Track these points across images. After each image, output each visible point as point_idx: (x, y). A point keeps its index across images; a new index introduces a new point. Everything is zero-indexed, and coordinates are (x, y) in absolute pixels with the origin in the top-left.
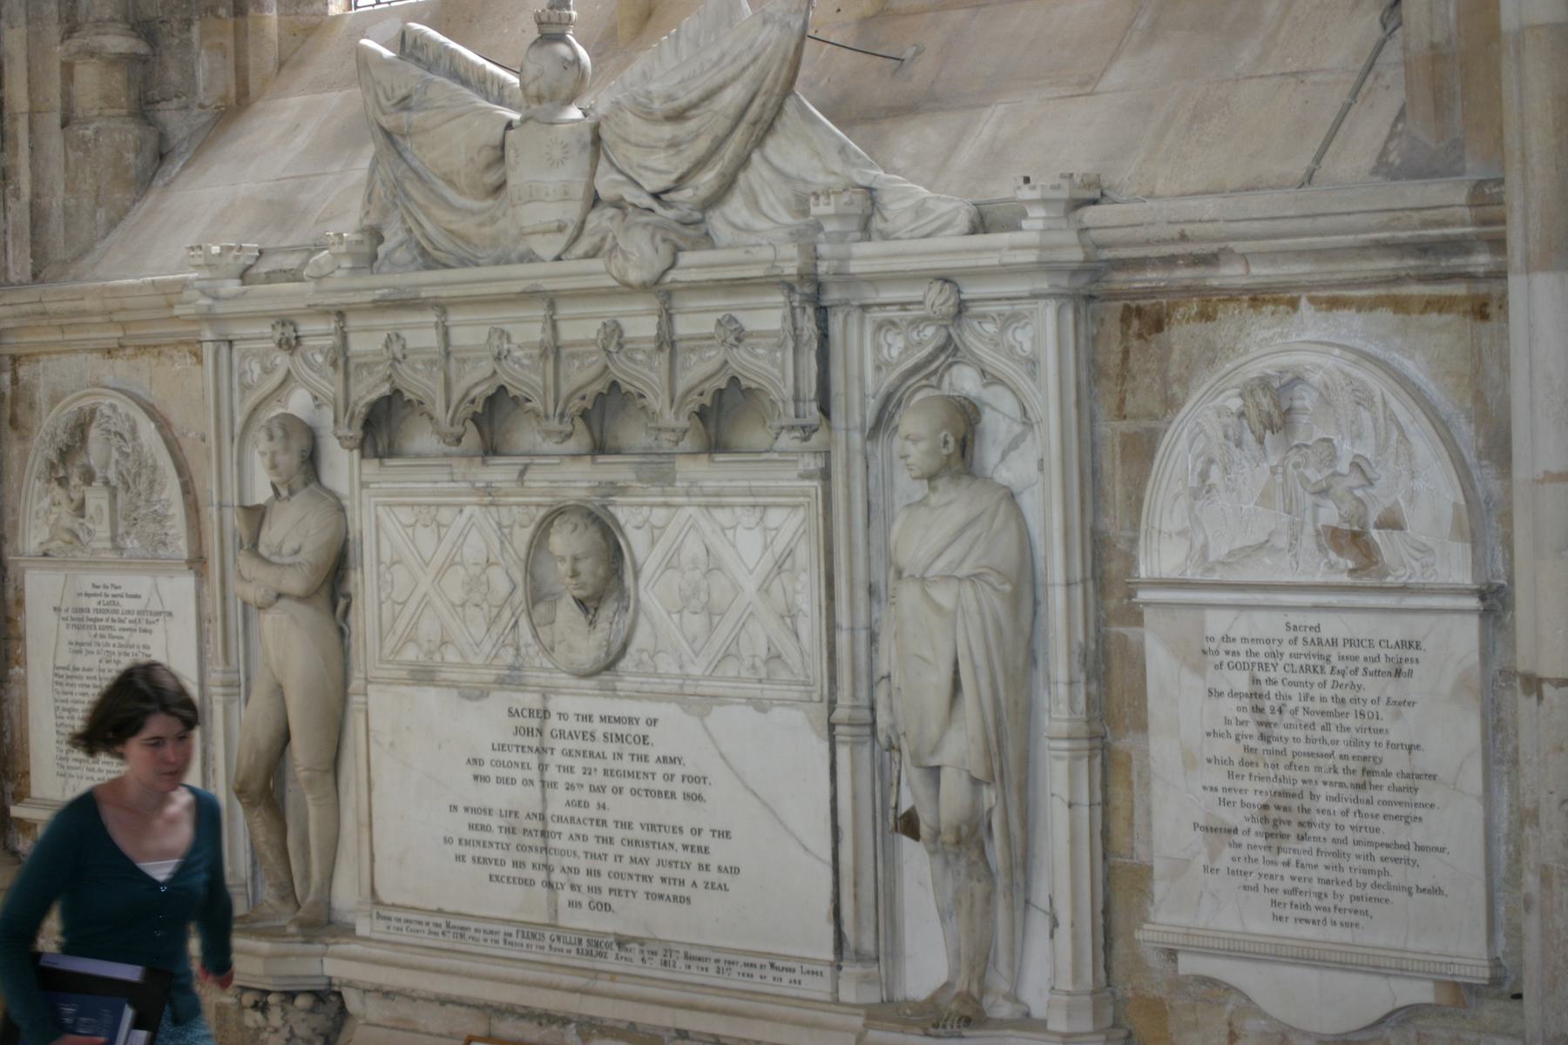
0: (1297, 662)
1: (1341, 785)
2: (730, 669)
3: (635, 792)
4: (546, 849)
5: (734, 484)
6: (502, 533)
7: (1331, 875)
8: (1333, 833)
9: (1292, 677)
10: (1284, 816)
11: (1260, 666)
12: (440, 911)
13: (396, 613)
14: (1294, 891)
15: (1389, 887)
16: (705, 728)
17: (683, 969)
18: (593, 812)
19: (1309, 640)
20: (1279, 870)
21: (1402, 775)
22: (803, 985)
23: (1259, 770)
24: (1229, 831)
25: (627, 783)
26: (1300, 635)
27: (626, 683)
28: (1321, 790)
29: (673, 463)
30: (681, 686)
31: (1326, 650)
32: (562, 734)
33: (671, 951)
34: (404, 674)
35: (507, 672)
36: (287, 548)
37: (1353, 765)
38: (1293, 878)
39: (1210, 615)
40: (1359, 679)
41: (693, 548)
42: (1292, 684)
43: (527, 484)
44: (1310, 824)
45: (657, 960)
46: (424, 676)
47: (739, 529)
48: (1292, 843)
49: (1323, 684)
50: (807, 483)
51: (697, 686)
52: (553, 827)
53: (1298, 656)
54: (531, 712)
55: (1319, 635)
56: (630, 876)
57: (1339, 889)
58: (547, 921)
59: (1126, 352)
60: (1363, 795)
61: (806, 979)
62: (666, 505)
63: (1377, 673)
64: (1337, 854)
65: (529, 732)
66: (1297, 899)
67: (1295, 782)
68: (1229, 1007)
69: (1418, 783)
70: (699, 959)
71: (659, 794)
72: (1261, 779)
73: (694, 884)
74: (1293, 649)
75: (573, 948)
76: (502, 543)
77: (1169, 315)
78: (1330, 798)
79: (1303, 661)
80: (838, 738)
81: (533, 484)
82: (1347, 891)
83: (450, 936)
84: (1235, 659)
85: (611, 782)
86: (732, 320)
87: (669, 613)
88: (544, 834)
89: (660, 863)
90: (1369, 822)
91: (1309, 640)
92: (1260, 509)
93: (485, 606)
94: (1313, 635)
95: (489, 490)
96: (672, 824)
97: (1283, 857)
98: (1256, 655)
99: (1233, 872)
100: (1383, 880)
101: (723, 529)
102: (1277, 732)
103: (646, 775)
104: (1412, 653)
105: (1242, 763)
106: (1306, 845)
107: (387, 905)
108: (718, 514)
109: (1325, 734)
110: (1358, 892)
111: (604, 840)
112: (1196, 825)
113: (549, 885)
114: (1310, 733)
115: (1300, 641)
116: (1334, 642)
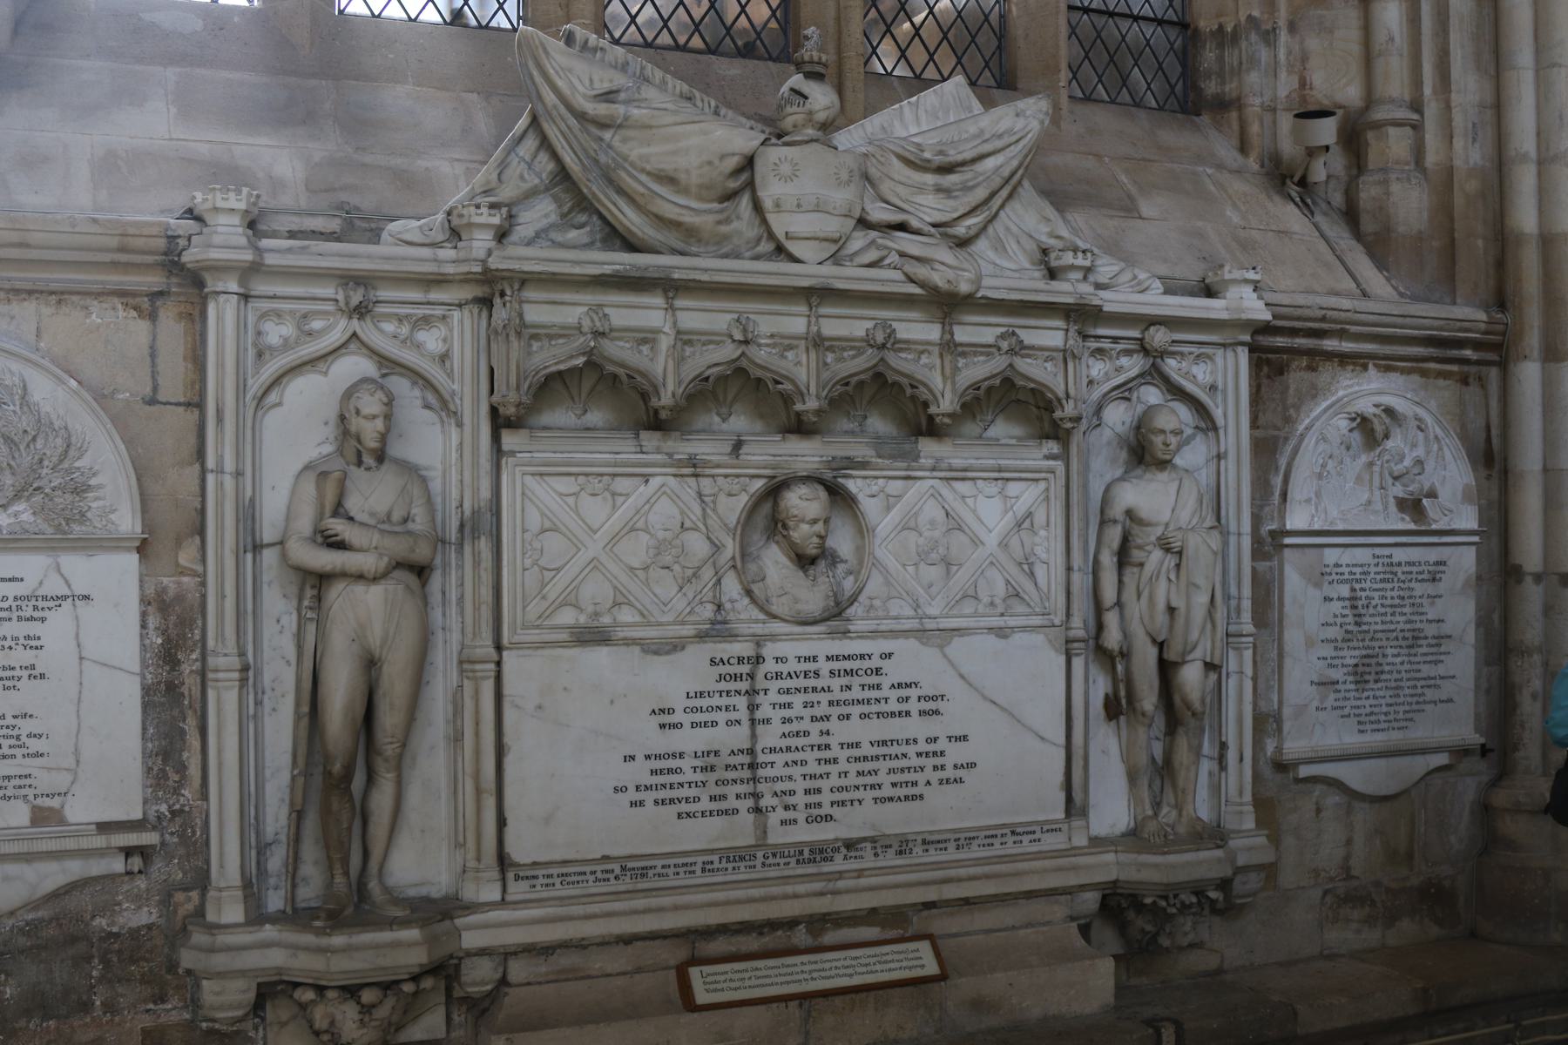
0: (1378, 577)
1: (1401, 647)
3: (863, 716)
6: (703, 502)
8: (1395, 676)
9: (1375, 586)
10: (1367, 669)
12: (606, 858)
13: (546, 580)
14: (1372, 714)
15: (1425, 702)
16: (945, 656)
17: (921, 853)
18: (815, 739)
21: (1434, 637)
23: (1355, 644)
25: (856, 710)
26: (1381, 561)
27: (858, 626)
28: (1389, 651)
29: (916, 442)
31: (1395, 569)
32: (778, 676)
33: (907, 841)
34: (564, 636)
36: (396, 517)
37: (1407, 634)
39: (1327, 551)
40: (1413, 585)
41: (932, 511)
44: (1382, 672)
45: (891, 852)
46: (592, 636)
47: (980, 497)
48: (1371, 685)
49: (1392, 589)
50: (1051, 463)
53: (1378, 573)
54: (740, 660)
56: (857, 787)
57: (1396, 708)
58: (753, 843)
60: (1413, 651)
63: (1423, 580)
64: (1397, 688)
65: (736, 677)
66: (1373, 718)
68: (1317, 793)
69: (1442, 641)
71: (893, 714)
75: (793, 860)
76: (704, 509)
77: (1288, 366)
78: (1394, 656)
79: (1382, 576)
81: (749, 457)
82: (1401, 709)
83: (628, 879)
85: (836, 711)
86: (1014, 334)
87: (904, 565)
89: (891, 771)
90: (1415, 667)
93: (676, 568)
95: (692, 462)
97: (1366, 694)
100: (1421, 699)
102: (1366, 619)
104: (1441, 568)
105: (1344, 640)
106: (1379, 685)
107: (524, 865)
108: (958, 485)
110: (1407, 708)
111: (827, 761)
112: (1312, 682)
113: (757, 810)
116: (1400, 564)
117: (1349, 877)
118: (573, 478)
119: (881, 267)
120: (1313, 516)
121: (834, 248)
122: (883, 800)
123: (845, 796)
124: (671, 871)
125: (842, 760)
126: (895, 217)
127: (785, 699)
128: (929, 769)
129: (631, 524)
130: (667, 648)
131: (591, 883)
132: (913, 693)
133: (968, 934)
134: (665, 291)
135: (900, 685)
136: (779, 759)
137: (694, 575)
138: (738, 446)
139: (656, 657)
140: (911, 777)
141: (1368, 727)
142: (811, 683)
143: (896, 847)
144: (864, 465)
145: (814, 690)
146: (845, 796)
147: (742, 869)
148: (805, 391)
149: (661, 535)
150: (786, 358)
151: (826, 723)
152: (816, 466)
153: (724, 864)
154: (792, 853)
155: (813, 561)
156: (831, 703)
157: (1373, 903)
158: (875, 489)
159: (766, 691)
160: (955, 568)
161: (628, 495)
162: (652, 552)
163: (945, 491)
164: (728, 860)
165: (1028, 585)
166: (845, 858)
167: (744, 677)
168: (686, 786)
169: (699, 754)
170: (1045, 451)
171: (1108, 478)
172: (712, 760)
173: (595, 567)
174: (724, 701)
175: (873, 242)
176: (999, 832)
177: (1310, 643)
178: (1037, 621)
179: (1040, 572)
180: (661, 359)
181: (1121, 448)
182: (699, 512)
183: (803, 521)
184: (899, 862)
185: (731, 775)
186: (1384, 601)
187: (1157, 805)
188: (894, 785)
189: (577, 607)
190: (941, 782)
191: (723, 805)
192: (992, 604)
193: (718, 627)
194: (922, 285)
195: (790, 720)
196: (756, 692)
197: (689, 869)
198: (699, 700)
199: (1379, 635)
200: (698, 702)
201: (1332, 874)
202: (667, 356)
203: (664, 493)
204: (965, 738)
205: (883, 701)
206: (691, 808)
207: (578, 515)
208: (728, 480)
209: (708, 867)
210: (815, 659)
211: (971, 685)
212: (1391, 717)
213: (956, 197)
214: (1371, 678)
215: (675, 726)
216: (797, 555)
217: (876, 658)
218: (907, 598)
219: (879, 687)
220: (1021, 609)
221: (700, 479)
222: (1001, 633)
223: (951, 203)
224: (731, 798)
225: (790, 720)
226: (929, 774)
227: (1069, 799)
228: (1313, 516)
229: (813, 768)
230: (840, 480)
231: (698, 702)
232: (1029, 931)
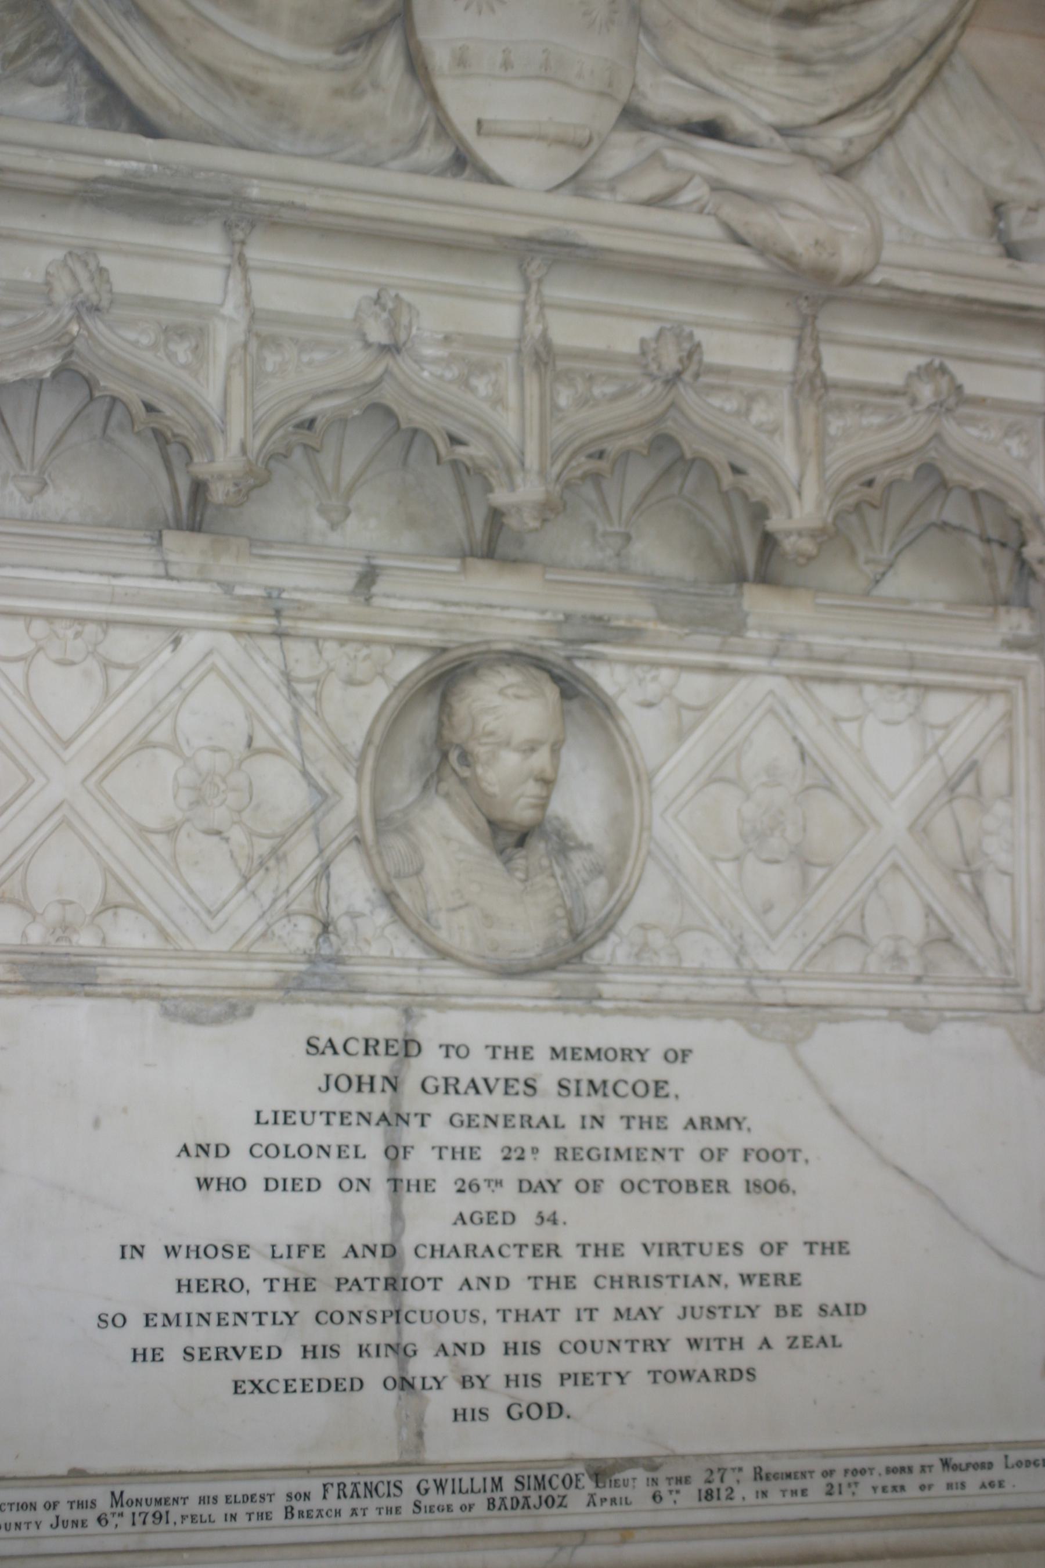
3: (631, 1186)
4: (398, 1314)
5: (870, 644)
6: (295, 694)
12: (77, 1475)
16: (800, 1063)
17: (751, 1498)
18: (526, 1231)
22: (1008, 1488)
25: (614, 1172)
29: (739, 595)
32: (450, 1085)
33: (722, 1470)
35: (303, 967)
43: (376, 601)
45: (689, 1493)
50: (1018, 656)
52: (413, 1267)
54: (370, 1047)
56: (615, 1345)
58: (395, 1458)
62: (721, 670)
65: (361, 1084)
70: (789, 1476)
71: (691, 1186)
73: (766, 1342)
75: (480, 1501)
76: (296, 711)
81: (393, 603)
83: (125, 1524)
85: (570, 1172)
86: (943, 370)
87: (713, 860)
88: (391, 1283)
89: (687, 1312)
93: (237, 835)
96: (716, 1239)
101: (836, 720)
103: (659, 1153)
108: (825, 693)
111: (552, 1283)
113: (404, 1383)
118: (20, 624)
119: (674, 208)
121: (574, 162)
123: (587, 1362)
124: (219, 1510)
125: (585, 1283)
126: (701, 109)
127: (463, 1137)
128: (766, 1313)
129: (141, 731)
130: (216, 1009)
131: (45, 1529)
132: (733, 1140)
134: (228, 227)
135: (705, 1122)
136: (452, 1270)
137: (274, 851)
138: (368, 577)
139: (191, 1030)
140: (729, 1328)
142: (520, 1105)
143: (698, 1482)
144: (631, 635)
145: (526, 1121)
146: (587, 1362)
147: (372, 1514)
148: (515, 462)
149: (205, 760)
150: (473, 390)
151: (550, 1196)
152: (531, 631)
153: (333, 1501)
154: (478, 1484)
155: (522, 839)
156: (561, 1153)
158: (652, 690)
159: (423, 1118)
160: (819, 873)
161: (135, 669)
162: (185, 797)
163: (797, 705)
164: (342, 1494)
166: (591, 1502)
167: (378, 1083)
168: (252, 1320)
169: (282, 1250)
172: (307, 1265)
173: (64, 821)
174: (333, 1136)
175: (655, 156)
178: (986, 997)
179: (996, 892)
180: (216, 374)
182: (285, 715)
183: (507, 744)
184: (707, 1514)
185: (349, 1301)
188: (694, 1343)
189: (23, 905)
191: (330, 1369)
192: (897, 957)
193: (324, 968)
194: (762, 251)
195: (474, 1186)
196: (402, 1119)
197: (257, 1507)
198: (281, 1128)
200: (280, 1135)
202: (229, 367)
203: (213, 668)
204: (841, 1247)
205: (670, 1156)
206: (262, 1370)
207: (33, 707)
208: (349, 649)
209: (299, 1505)
210: (527, 1053)
211: (852, 1129)
213: (822, 75)
215: (230, 1184)
216: (491, 822)
217: (654, 1058)
220: (955, 969)
221: (289, 644)
223: (812, 88)
224: (350, 1352)
225: (474, 1186)
226: (766, 1324)
229: (522, 1296)
230: (580, 665)
231: (280, 1135)
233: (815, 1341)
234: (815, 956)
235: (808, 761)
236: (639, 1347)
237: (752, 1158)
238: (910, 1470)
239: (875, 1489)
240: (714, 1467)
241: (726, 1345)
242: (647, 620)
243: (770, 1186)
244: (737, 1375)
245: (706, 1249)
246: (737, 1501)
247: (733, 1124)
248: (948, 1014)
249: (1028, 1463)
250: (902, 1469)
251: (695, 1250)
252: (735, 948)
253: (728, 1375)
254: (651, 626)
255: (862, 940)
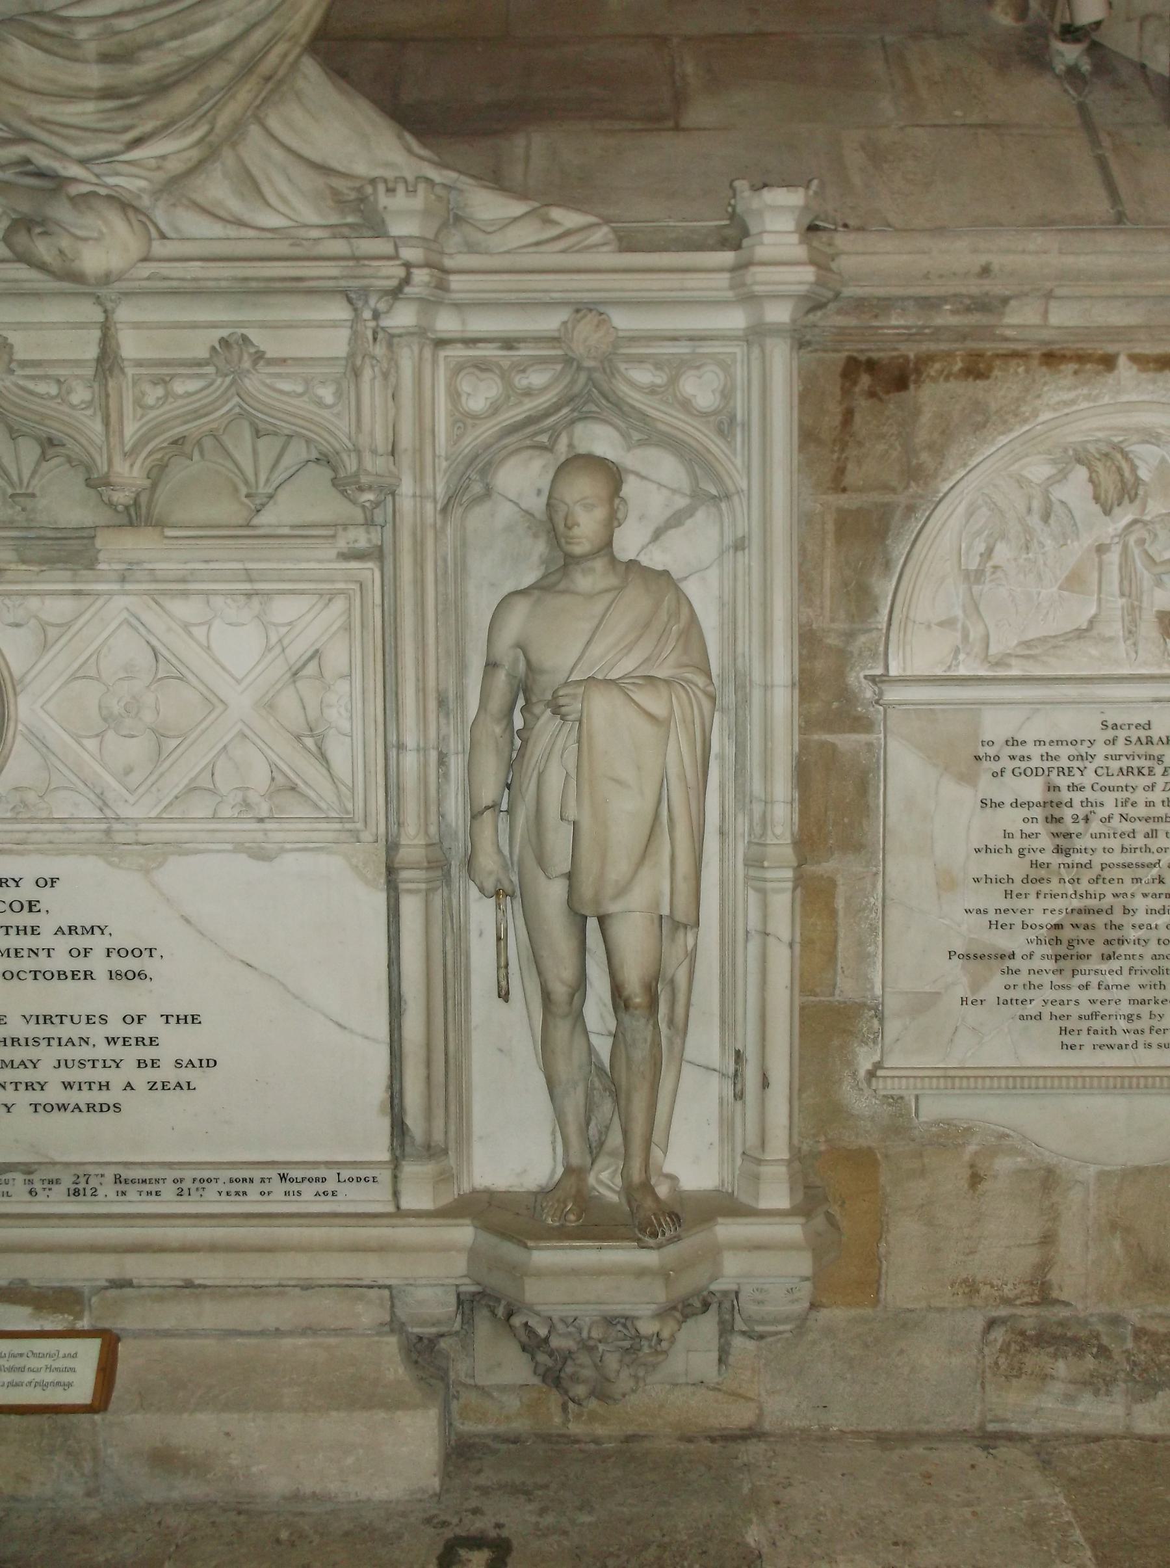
0: (1114, 765)
2: (200, 807)
7: (1148, 994)
9: (1105, 781)
11: (1061, 771)
14: (1094, 1015)
16: (153, 885)
17: (112, 1196)
19: (1134, 739)
20: (1074, 994)
22: (340, 1197)
23: (1055, 886)
24: (1002, 957)
26: (1122, 734)
28: (1140, 903)
30: (108, 832)
33: (88, 1177)
38: (1092, 1002)
42: (1103, 789)
44: (1121, 941)
45: (59, 1191)
47: (217, 624)
48: (1094, 964)
51: (137, 832)
53: (1118, 757)
55: (1148, 733)
59: (848, 417)
61: (344, 1189)
62: (77, 593)
67: (1102, 896)
68: (972, 1148)
70: (144, 1181)
71: (62, 975)
72: (1054, 896)
73: (129, 1084)
74: (1110, 750)
77: (918, 371)
78: (1151, 911)
79: (1124, 763)
80: (402, 886)
84: (1023, 765)
87: (77, 738)
91: (1134, 739)
92: (1065, 593)
94: (1143, 734)
96: (84, 1012)
97: (1080, 979)
98: (1056, 758)
99: (1006, 1002)
101: (186, 627)
102: (1078, 843)
105: (1027, 880)
106: (1115, 964)
109: (1149, 842)
112: (951, 954)
114: (1127, 842)
115: (1121, 741)
117: (1045, 1298)
120: (957, 651)
122: (49, 1108)
132: (98, 943)
133: (192, 1334)
135: (72, 930)
140: (100, 1075)
141: (1084, 1039)
143: (67, 1182)
157: (1103, 1352)
160: (173, 743)
165: (312, 771)
170: (342, 544)
171: (509, 587)
176: (257, 1174)
177: (947, 883)
179: (338, 753)
181: (536, 536)
186: (1129, 811)
187: (595, 1150)
188: (68, 1085)
190: (152, 1087)
199: (1117, 873)
201: (1008, 1291)
212: (1144, 1024)
214: (1095, 950)
218: (86, 790)
219: (34, 930)
222: (261, 855)
227: (399, 1128)
228: (957, 651)
232: (301, 1341)
233: (172, 1086)
234: (171, 804)
235: (160, 658)
236: (22, 1087)
237: (114, 955)
238: (251, 1181)
239: (220, 1193)
240: (81, 1174)
241: (95, 1087)
242: (10, 562)
243: (130, 975)
244: (105, 1108)
245: (76, 1020)
246: (101, 1197)
247: (96, 930)
248: (288, 846)
249: (359, 1180)
250: (244, 1180)
251: (66, 1020)
252: (100, 803)
253: (97, 1108)
254: (13, 566)
255: (214, 792)
